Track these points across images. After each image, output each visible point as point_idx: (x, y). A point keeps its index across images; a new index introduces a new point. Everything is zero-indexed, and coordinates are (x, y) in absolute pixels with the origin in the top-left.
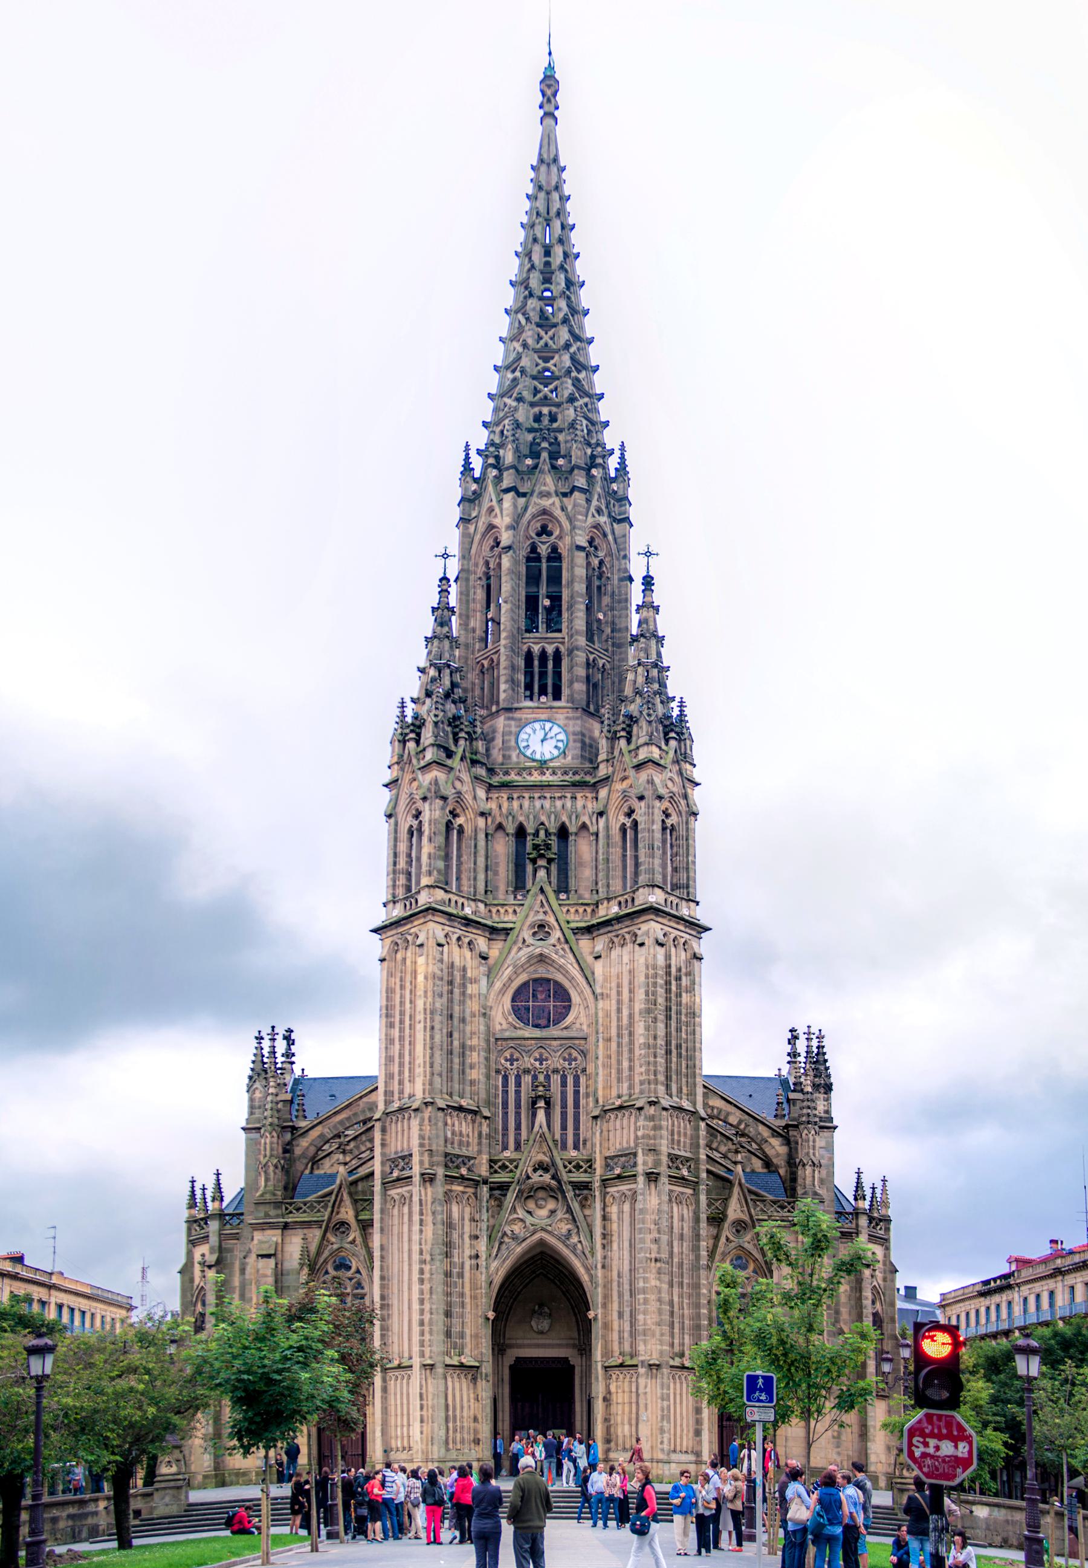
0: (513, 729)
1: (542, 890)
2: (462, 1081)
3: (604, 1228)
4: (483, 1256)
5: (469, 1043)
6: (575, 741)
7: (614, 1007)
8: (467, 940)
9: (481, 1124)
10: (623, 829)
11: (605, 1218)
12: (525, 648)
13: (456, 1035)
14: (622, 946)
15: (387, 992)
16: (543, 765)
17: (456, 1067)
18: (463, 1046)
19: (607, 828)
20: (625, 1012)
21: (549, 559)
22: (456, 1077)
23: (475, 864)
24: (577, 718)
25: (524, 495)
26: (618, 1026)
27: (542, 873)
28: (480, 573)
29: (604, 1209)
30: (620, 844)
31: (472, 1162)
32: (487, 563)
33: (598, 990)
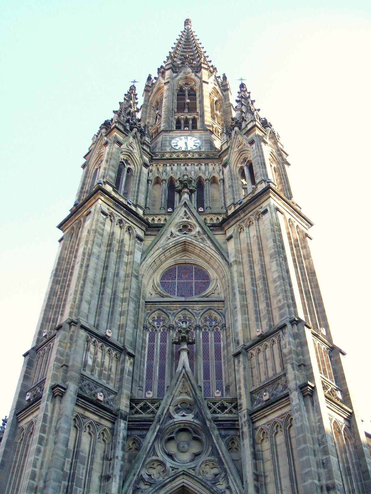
0: (168, 139)
2: (110, 321)
3: (256, 466)
6: (206, 143)
9: (124, 361)
11: (256, 456)
12: (176, 117)
13: (109, 284)
15: (59, 259)
17: (106, 309)
18: (114, 293)
19: (230, 171)
20: (257, 268)
21: (189, 91)
22: (105, 315)
23: (138, 188)
24: (207, 135)
25: (176, 72)
26: (252, 279)
27: (186, 196)
29: (254, 445)
31: (112, 396)
32: (157, 102)
33: (232, 259)
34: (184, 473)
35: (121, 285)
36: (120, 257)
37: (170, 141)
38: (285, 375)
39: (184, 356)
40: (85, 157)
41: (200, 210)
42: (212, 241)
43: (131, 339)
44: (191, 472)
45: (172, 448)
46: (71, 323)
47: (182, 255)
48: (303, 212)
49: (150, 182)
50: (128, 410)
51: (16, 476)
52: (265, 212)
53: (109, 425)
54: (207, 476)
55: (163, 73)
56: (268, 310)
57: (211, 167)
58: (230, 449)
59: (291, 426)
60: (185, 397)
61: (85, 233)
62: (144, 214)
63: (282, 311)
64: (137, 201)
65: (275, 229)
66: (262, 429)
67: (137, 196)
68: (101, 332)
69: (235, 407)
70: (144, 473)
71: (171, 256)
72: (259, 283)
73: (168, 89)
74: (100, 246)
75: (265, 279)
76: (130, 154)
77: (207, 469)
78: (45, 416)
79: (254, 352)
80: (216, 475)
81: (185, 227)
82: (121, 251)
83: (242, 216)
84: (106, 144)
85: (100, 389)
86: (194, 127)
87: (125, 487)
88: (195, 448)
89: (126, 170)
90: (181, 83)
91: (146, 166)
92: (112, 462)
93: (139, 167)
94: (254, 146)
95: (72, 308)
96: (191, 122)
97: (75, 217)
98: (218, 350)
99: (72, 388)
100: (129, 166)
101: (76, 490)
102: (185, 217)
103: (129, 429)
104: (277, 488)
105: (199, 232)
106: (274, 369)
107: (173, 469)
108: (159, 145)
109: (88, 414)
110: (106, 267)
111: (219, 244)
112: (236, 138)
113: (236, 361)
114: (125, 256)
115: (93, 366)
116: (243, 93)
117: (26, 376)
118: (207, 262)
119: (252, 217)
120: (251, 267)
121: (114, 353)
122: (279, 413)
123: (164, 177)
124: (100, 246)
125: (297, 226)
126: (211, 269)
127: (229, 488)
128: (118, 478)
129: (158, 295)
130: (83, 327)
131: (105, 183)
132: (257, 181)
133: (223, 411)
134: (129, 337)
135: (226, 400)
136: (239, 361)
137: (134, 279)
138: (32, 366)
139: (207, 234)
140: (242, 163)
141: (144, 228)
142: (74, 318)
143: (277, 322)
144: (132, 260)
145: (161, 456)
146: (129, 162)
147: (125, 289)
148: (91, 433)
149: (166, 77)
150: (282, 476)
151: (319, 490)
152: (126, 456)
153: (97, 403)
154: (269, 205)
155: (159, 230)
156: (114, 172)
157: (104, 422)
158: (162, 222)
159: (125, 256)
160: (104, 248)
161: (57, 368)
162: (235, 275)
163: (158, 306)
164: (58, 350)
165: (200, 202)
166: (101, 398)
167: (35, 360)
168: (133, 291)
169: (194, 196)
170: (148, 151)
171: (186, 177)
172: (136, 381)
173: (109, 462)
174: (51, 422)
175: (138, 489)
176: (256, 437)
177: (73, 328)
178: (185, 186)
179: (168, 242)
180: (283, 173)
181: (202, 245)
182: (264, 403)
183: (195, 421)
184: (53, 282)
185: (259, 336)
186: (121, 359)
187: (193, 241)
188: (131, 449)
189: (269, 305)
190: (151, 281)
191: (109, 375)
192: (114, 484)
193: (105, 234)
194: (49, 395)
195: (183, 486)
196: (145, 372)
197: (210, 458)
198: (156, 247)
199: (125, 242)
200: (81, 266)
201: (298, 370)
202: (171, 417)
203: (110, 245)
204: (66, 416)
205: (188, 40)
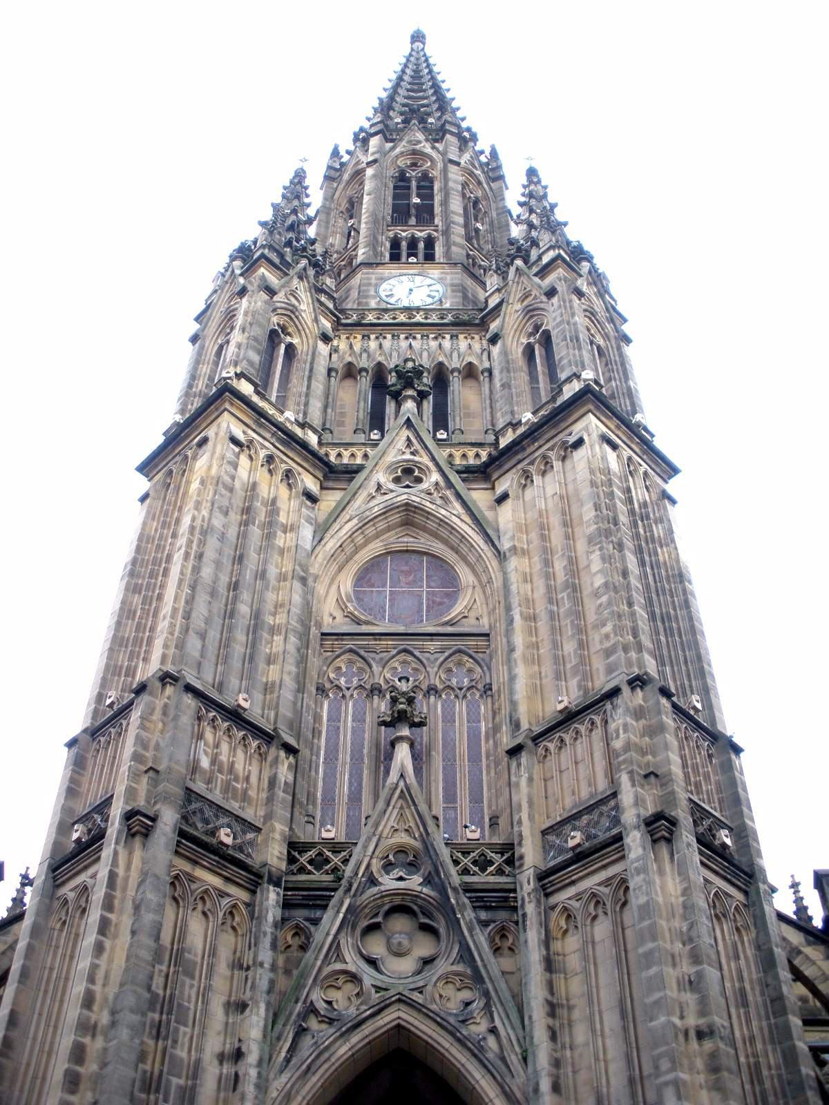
0: (373, 281)
1: (408, 423)
4: (252, 1057)
5: (270, 620)
6: (453, 291)
7: (538, 566)
8: (284, 467)
9: (276, 761)
10: (529, 352)
11: (550, 965)
12: (391, 234)
13: (245, 596)
14: (544, 473)
15: (140, 539)
16: (408, 310)
17: (238, 649)
18: (257, 616)
19: (505, 353)
20: (559, 566)
21: (419, 180)
22: (236, 663)
23: (309, 387)
24: (457, 273)
25: (392, 141)
26: (548, 587)
27: (409, 405)
28: (343, 208)
29: (547, 942)
30: (525, 368)
31: (250, 836)
33: (505, 545)
34: (402, 1000)
35: (271, 597)
36: (269, 537)
37: (377, 286)
38: (615, 795)
39: (403, 753)
40: (197, 319)
41: (439, 436)
42: (464, 504)
43: (289, 714)
44: (416, 996)
45: (376, 946)
46: (166, 678)
47: (401, 532)
48: (658, 443)
49: (333, 374)
50: (283, 866)
51: (53, 999)
52: (579, 443)
53: (244, 895)
54: (449, 1005)
55: (365, 142)
56: (581, 657)
57: (463, 343)
58: (497, 950)
59: (625, 904)
60: (403, 838)
61: (195, 485)
62: (320, 443)
63: (612, 659)
64: (305, 414)
65: (599, 481)
66: (565, 909)
67: (306, 404)
68: (227, 700)
69: (510, 862)
70: (318, 997)
71: (377, 536)
72: (563, 598)
73: (374, 176)
74: (226, 514)
75: (574, 589)
76: (292, 312)
77: (449, 991)
78: (112, 876)
79: (551, 746)
80: (468, 1004)
81: (408, 471)
82: (270, 524)
83: (529, 451)
84: (243, 292)
85: (226, 820)
86: (429, 257)
87: (279, 1027)
88: (424, 946)
89: (283, 347)
90: (401, 163)
91: (326, 338)
92: (250, 973)
93: (310, 341)
94: (555, 300)
95: (166, 646)
96: (421, 245)
97: (174, 449)
98: (474, 737)
99: (169, 818)
100: (288, 339)
101: (177, 1030)
102: (408, 451)
103: (287, 905)
104: (593, 1031)
105: (437, 484)
106: (592, 782)
107: (378, 989)
108: (354, 294)
109: (200, 873)
110: (240, 559)
111: (478, 508)
112: (518, 283)
113: (514, 764)
114: (279, 533)
115: (212, 772)
116: (532, 187)
117: (72, 790)
118: (452, 548)
119: (550, 453)
120: (547, 563)
121: (255, 744)
122: (603, 876)
123: (364, 363)
124: (226, 514)
125: (646, 473)
126: (462, 563)
127: (493, 1031)
128: (263, 1007)
129: (347, 619)
130: (189, 688)
131: (239, 376)
132: (563, 376)
133: (483, 869)
134: (286, 711)
135: (490, 846)
136: (519, 765)
137: (297, 585)
138: (84, 768)
139: (455, 488)
140: (530, 335)
141: (320, 476)
142: (169, 668)
143: (602, 683)
144: (294, 544)
145: (352, 962)
146: (290, 330)
147: (277, 606)
148: (208, 913)
149: (371, 150)
150: (604, 1007)
151: (681, 1037)
152: (281, 961)
153: (218, 851)
154: (586, 429)
155: (351, 480)
156: (259, 352)
157: (232, 890)
158: (359, 461)
159: (279, 533)
160: (235, 517)
161: (135, 776)
162: (513, 577)
163: (349, 644)
164: (138, 737)
165: (441, 420)
166: (228, 841)
167: (89, 756)
168: (295, 610)
169: (428, 406)
170: (331, 306)
171: (410, 365)
172: (301, 804)
173: (244, 974)
174: (124, 889)
175: (305, 1030)
176: (552, 925)
177: (169, 690)
178: (409, 384)
179: (372, 504)
180: (617, 358)
181: (443, 512)
182: (570, 855)
183: (425, 890)
184: (127, 589)
185: (561, 712)
186: (270, 758)
187: (424, 502)
188: (289, 946)
189: (582, 645)
190: (334, 587)
191: (245, 791)
192: (254, 1018)
193: (237, 484)
194: (119, 832)
195: (399, 1026)
196: (320, 784)
197: (455, 968)
198: (345, 516)
199: (279, 504)
200: (187, 555)
201: (642, 786)
202: (373, 881)
203: (247, 510)
204: (156, 876)
205: (417, 74)
